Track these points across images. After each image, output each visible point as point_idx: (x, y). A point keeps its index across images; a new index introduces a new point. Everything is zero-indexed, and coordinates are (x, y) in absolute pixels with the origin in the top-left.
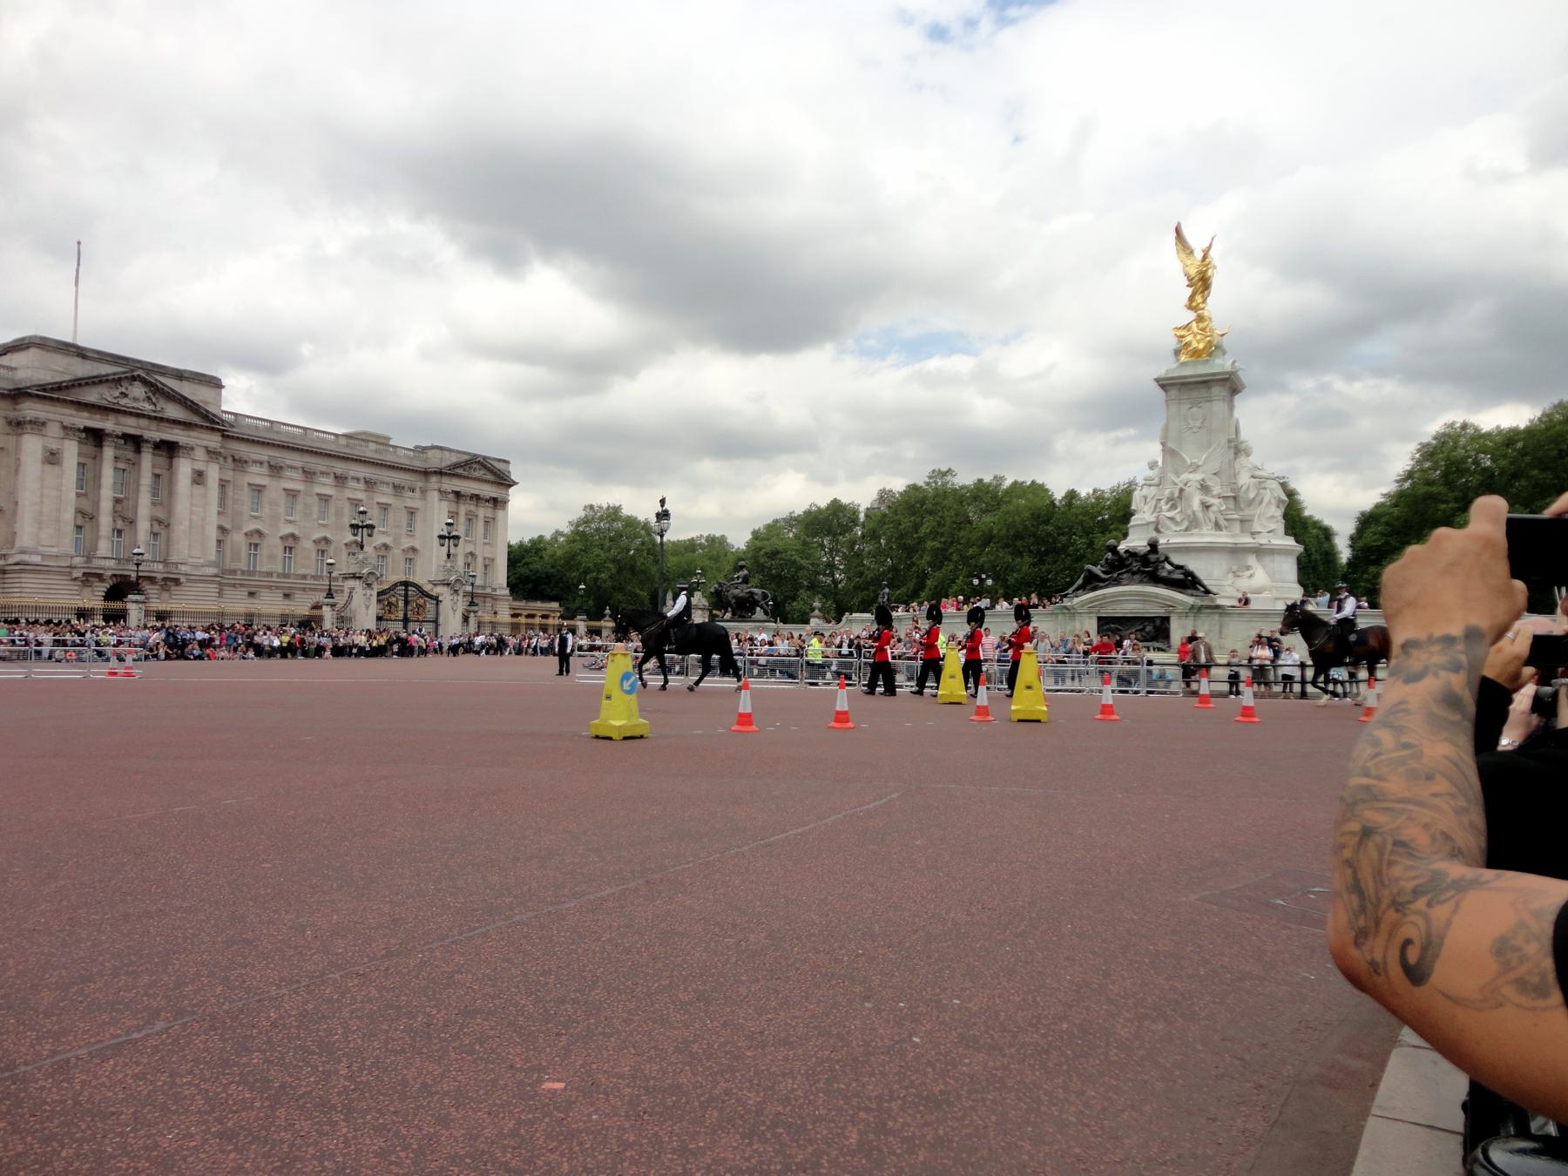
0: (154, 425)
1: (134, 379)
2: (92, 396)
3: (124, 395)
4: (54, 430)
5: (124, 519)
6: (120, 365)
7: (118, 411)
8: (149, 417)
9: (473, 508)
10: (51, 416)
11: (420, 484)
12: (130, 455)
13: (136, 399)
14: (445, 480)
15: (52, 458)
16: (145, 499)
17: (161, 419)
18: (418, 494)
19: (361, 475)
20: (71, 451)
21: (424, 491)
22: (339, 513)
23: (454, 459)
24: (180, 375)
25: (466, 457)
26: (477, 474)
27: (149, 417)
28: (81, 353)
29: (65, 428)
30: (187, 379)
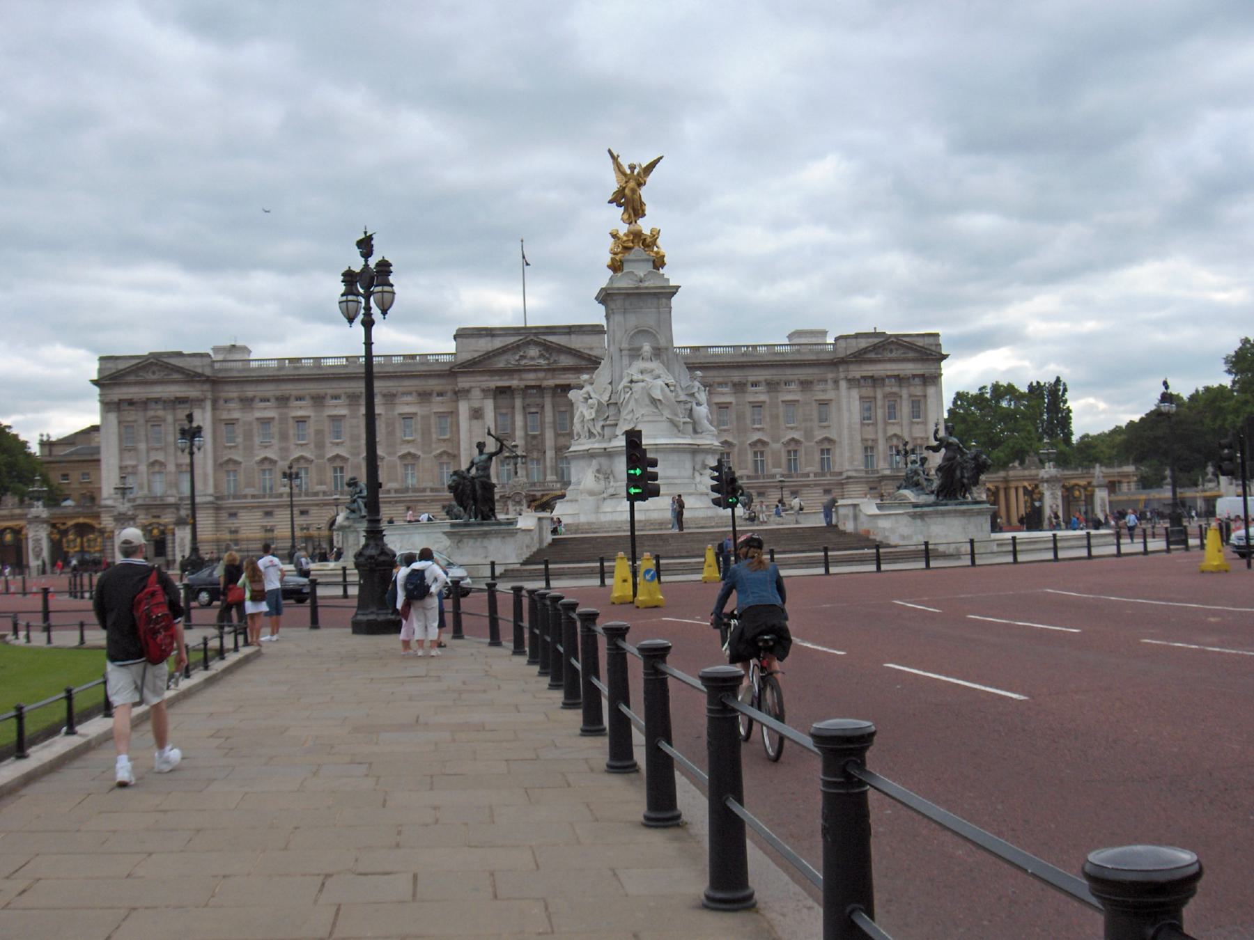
0: (549, 375)
1: (528, 343)
2: (501, 363)
3: (522, 357)
4: (476, 393)
5: (539, 451)
6: (520, 334)
7: (520, 371)
8: (544, 370)
9: (895, 389)
10: (473, 384)
11: (830, 376)
12: (538, 400)
13: (532, 359)
14: (852, 367)
15: (477, 414)
16: (549, 435)
17: (554, 370)
18: (830, 385)
19: (761, 378)
20: (489, 405)
21: (836, 382)
22: (740, 417)
23: (863, 344)
24: (570, 330)
25: (876, 340)
26: (894, 355)
27: (544, 370)
28: (490, 333)
29: (483, 390)
30: (574, 333)
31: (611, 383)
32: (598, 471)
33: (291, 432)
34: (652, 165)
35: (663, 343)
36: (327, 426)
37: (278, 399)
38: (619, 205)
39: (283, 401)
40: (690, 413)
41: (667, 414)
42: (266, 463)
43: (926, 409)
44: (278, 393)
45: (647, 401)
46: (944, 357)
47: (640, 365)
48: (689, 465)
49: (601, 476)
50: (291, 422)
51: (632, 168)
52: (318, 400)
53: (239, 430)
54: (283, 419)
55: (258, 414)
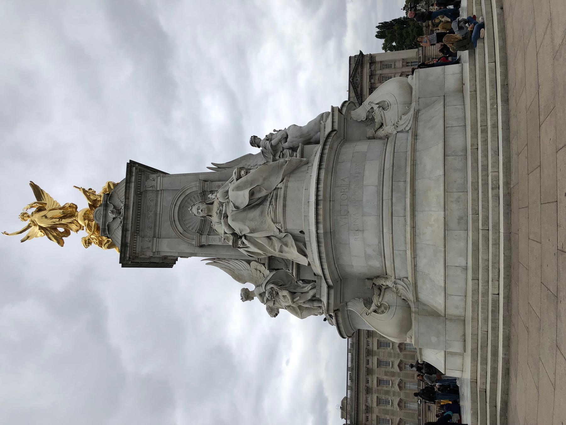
31: (249, 262)
32: (368, 303)
33: (385, 388)
34: (38, 192)
35: (195, 187)
36: (383, 369)
37: (367, 393)
38: (67, 233)
39: (368, 391)
40: (293, 149)
41: (276, 181)
42: (401, 404)
43: (387, 61)
44: (365, 392)
45: (255, 213)
46: (361, 52)
47: (215, 218)
48: (362, 147)
49: (376, 301)
50: (378, 388)
51: (24, 216)
52: (369, 372)
53: (383, 416)
54: (378, 391)
55: (375, 404)
